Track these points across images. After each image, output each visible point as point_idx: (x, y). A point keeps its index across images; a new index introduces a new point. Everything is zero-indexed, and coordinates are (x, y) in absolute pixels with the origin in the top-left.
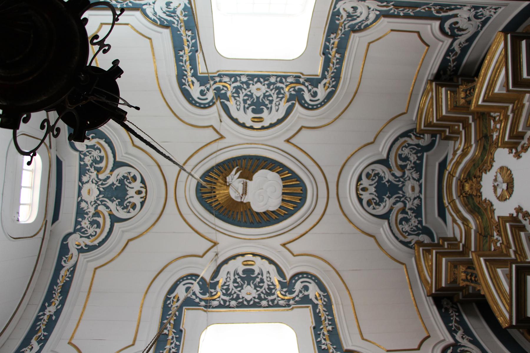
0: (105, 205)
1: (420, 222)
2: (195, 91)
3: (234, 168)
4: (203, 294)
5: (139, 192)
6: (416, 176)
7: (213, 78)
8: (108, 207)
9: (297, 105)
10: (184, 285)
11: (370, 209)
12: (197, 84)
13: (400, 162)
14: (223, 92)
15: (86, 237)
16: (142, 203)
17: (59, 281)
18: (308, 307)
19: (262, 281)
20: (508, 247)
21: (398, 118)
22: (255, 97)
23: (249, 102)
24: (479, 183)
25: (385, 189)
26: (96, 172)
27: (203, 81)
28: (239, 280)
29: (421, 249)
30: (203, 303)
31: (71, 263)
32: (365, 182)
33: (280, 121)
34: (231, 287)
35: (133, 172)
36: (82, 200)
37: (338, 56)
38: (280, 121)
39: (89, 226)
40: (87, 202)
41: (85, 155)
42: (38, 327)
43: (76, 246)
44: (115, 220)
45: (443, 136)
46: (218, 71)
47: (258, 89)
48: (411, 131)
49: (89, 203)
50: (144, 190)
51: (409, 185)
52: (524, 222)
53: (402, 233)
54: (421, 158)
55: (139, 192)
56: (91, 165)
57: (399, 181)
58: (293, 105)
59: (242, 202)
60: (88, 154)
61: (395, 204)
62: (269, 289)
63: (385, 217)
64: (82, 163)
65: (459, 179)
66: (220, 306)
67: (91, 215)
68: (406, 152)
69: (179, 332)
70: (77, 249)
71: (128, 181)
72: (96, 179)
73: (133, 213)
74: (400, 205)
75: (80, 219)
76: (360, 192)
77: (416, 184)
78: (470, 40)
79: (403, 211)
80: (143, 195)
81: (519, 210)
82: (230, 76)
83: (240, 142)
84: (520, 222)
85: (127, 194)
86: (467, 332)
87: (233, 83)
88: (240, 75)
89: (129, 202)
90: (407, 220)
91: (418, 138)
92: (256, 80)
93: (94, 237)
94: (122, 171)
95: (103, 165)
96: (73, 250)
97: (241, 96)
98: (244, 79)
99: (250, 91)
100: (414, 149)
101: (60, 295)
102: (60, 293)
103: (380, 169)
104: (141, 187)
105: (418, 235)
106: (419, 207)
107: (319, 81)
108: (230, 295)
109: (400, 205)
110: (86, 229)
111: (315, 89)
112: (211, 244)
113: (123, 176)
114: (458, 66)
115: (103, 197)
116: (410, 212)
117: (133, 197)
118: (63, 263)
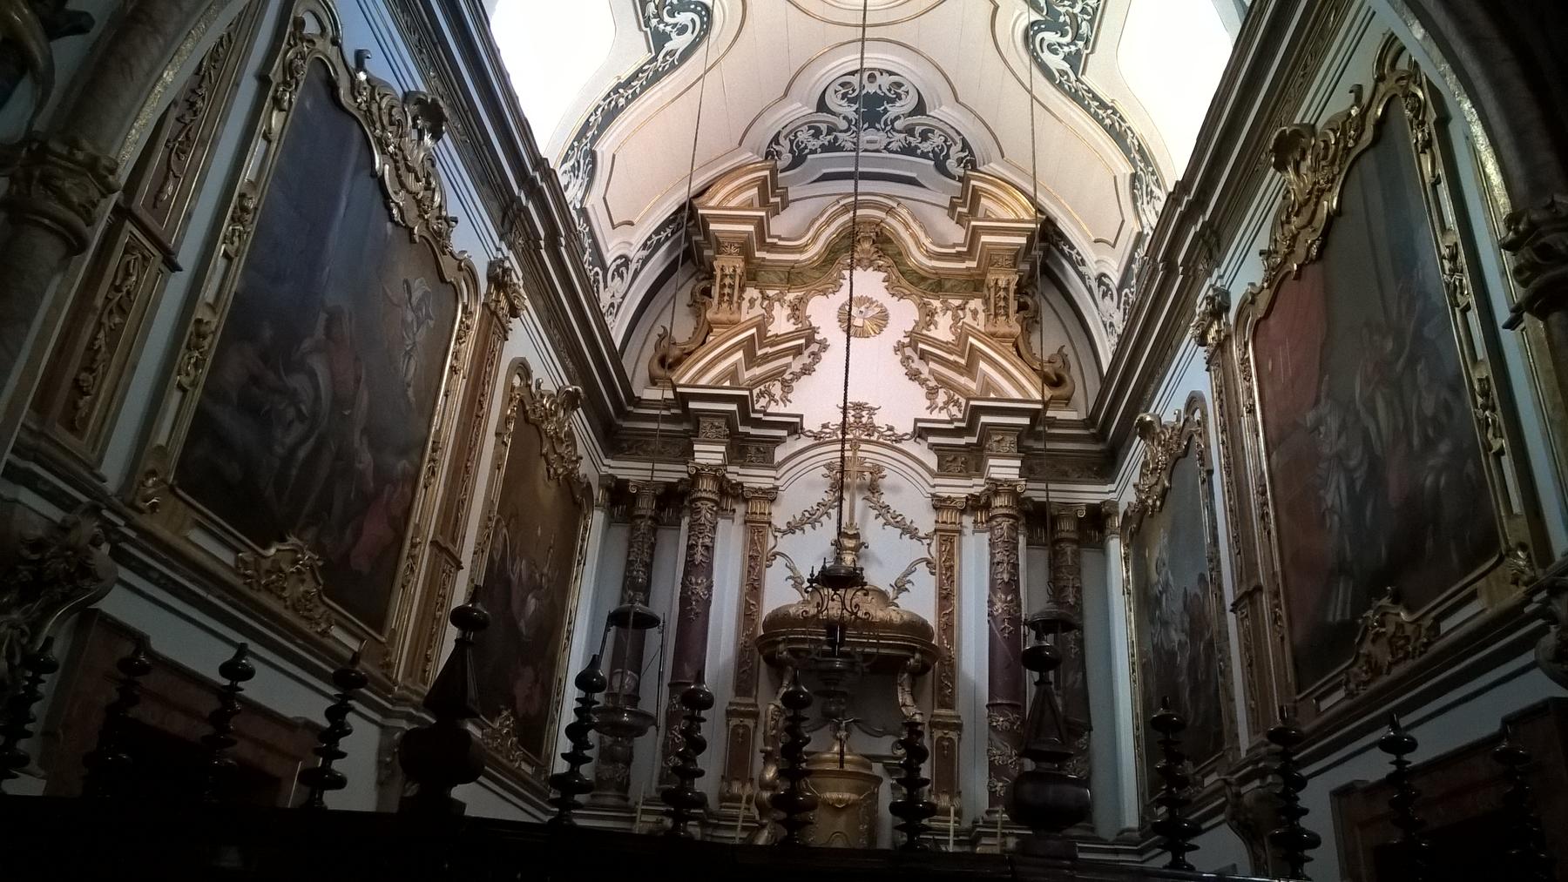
1: (813, 152)
9: (1035, 17)
11: (836, 86)
13: (918, 129)
25: (871, 109)
29: (767, 173)
32: (885, 81)
37: (1108, 121)
51: (880, 138)
52: (806, 353)
53: (795, 132)
54: (924, 155)
58: (1039, 10)
63: (822, 106)
68: (937, 140)
74: (843, 125)
81: (824, 346)
84: (807, 346)
86: (645, 261)
90: (817, 133)
91: (960, 161)
103: (909, 103)
105: (791, 151)
106: (840, 149)
107: (1074, 68)
109: (843, 125)
111: (1062, 55)
114: (1062, 252)
116: (830, 137)
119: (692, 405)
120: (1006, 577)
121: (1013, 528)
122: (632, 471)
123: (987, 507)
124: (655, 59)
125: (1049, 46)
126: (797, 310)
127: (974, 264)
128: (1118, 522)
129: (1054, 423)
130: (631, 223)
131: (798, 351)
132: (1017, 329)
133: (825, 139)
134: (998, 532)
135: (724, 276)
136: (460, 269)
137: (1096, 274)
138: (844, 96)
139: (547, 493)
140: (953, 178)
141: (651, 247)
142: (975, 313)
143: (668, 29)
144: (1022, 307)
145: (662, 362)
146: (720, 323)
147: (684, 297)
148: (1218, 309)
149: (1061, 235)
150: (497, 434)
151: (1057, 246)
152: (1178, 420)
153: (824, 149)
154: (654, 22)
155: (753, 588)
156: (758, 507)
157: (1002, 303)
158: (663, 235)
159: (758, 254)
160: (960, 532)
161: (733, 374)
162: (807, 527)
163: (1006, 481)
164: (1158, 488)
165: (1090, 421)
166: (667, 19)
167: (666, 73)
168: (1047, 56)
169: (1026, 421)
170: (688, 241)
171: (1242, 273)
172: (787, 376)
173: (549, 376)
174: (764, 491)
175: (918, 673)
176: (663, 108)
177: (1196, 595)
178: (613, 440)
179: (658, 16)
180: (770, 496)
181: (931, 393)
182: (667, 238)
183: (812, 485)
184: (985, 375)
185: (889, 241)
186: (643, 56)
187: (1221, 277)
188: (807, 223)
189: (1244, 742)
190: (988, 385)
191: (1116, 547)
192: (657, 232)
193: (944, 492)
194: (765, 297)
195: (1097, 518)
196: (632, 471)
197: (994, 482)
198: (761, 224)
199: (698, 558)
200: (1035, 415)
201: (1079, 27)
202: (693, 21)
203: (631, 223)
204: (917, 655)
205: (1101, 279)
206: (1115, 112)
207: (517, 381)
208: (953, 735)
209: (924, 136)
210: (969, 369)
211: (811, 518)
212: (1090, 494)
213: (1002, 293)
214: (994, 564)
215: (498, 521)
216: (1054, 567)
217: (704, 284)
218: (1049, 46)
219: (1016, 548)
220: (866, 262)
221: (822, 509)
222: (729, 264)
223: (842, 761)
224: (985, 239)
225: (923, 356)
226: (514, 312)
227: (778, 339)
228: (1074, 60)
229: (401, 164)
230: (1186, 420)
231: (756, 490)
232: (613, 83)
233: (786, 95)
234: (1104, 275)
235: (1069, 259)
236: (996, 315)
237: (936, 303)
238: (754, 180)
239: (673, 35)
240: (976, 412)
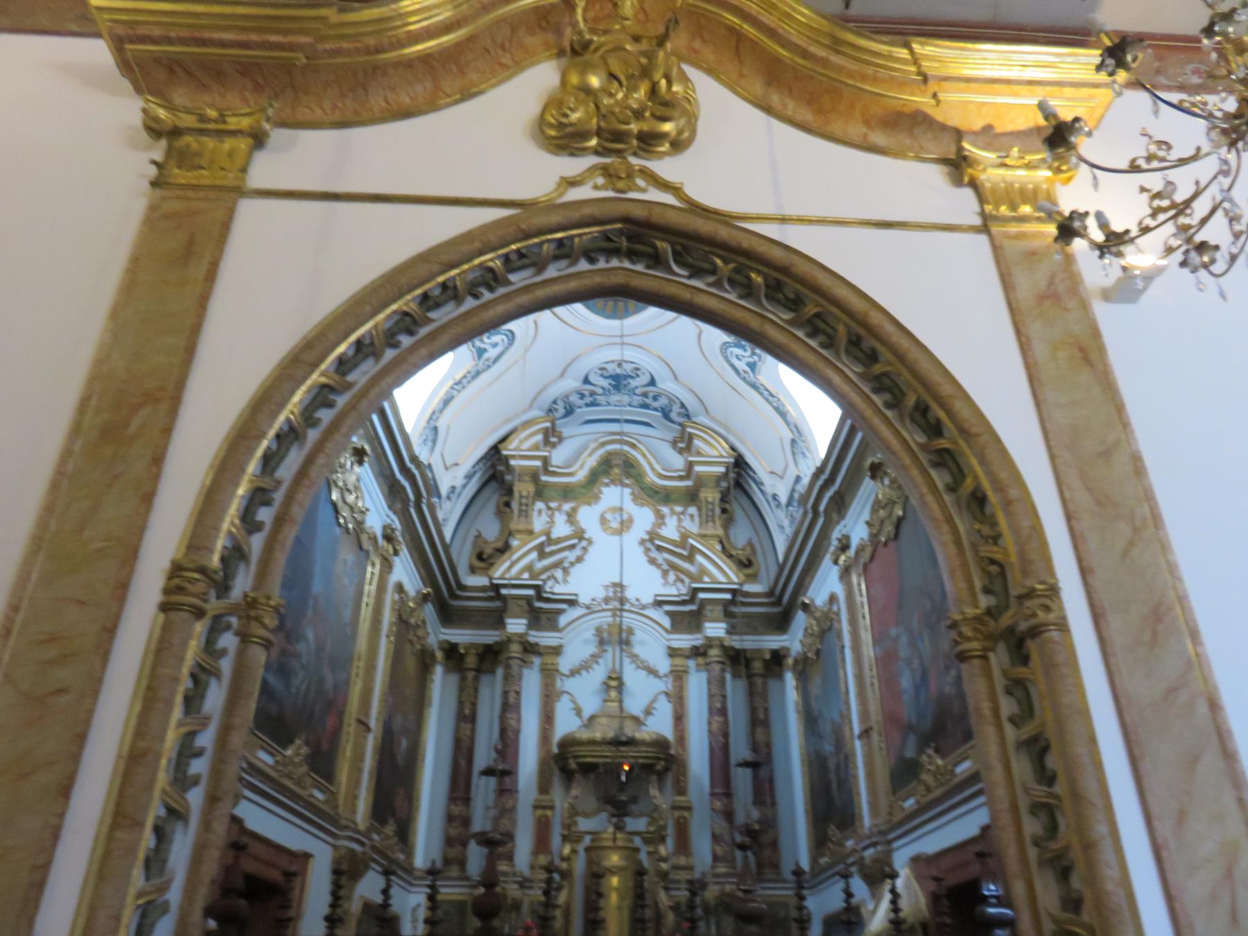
6: (635, 403)
13: (651, 395)
25: (618, 382)
29: (548, 424)
51: (626, 399)
52: (578, 548)
53: (567, 396)
54: (655, 409)
63: (586, 381)
74: (600, 391)
79: (592, 394)
86: (464, 486)
90: (582, 396)
91: (679, 414)
103: (645, 379)
106: (598, 405)
109: (600, 391)
119: (504, 591)
121: (723, 670)
122: (461, 636)
123: (704, 654)
126: (571, 517)
127: (689, 483)
128: (790, 661)
129: (748, 594)
130: (457, 464)
131: (573, 547)
132: (720, 532)
133: (588, 400)
135: (521, 497)
138: (602, 375)
140: (673, 422)
141: (469, 477)
142: (692, 516)
144: (724, 511)
145: (480, 557)
147: (491, 507)
153: (587, 405)
155: (548, 718)
156: (549, 659)
160: (686, 672)
161: (529, 568)
162: (584, 672)
165: (770, 594)
167: (484, 371)
169: (728, 596)
170: (495, 471)
171: (856, 527)
172: (566, 565)
174: (551, 647)
175: (661, 775)
178: (448, 615)
180: (557, 651)
181: (665, 574)
183: (586, 641)
185: (632, 466)
188: (576, 453)
189: (867, 821)
190: (703, 571)
191: (790, 679)
193: (675, 644)
194: (549, 508)
195: (777, 658)
196: (461, 636)
197: (709, 639)
198: (546, 461)
203: (457, 464)
204: (663, 761)
205: (775, 497)
208: (686, 814)
209: (655, 398)
210: (690, 559)
211: (585, 666)
212: (773, 642)
214: (711, 696)
216: (751, 694)
217: (506, 498)
222: (523, 488)
223: (615, 839)
224: (698, 468)
225: (659, 548)
226: (396, 553)
227: (560, 540)
235: (754, 479)
237: (665, 510)
240: (695, 591)
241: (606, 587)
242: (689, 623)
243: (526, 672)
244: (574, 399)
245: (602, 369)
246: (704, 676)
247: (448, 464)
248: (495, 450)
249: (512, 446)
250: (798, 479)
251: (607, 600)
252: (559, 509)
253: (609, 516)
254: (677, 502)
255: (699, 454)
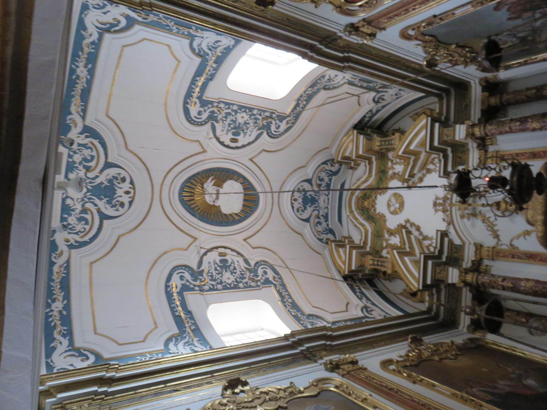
0: (93, 203)
1: (328, 225)
2: (194, 110)
3: (209, 177)
4: (195, 280)
5: (127, 193)
7: (211, 103)
8: (96, 205)
9: (265, 134)
10: (177, 274)
11: (298, 214)
12: (198, 104)
13: (319, 182)
14: (216, 115)
15: (74, 233)
16: (131, 203)
17: (54, 278)
18: (271, 286)
19: (235, 268)
20: (404, 244)
21: (322, 152)
22: (237, 123)
23: (232, 126)
24: (374, 201)
25: (309, 201)
26: (84, 171)
27: (204, 103)
28: (218, 268)
29: (333, 244)
30: (197, 288)
31: (63, 259)
33: (249, 144)
34: (214, 274)
35: (123, 174)
36: (67, 197)
37: (305, 103)
38: (249, 144)
39: (76, 222)
40: (72, 199)
41: (75, 153)
42: (53, 324)
43: (65, 243)
44: (104, 217)
45: (349, 167)
46: (219, 99)
47: (243, 117)
48: (328, 161)
49: (75, 200)
50: (132, 191)
52: (410, 229)
54: (330, 180)
55: (127, 193)
56: (80, 163)
57: (316, 195)
58: (262, 133)
59: (214, 205)
60: (78, 151)
61: (313, 211)
62: (241, 274)
63: (307, 220)
64: (70, 160)
65: (357, 197)
66: (210, 290)
67: (77, 211)
69: (189, 313)
70: (67, 245)
71: (118, 181)
72: (84, 177)
73: (122, 211)
75: (66, 216)
76: (293, 202)
77: (326, 197)
78: (384, 107)
79: (318, 217)
80: (131, 195)
81: (407, 221)
82: (226, 104)
83: (216, 156)
85: (116, 194)
87: (226, 109)
88: (233, 104)
89: (118, 201)
90: (319, 223)
91: (332, 165)
92: (243, 110)
93: (83, 234)
94: (112, 172)
95: (93, 164)
96: (62, 246)
97: (228, 120)
98: (235, 108)
99: (236, 118)
100: (327, 173)
101: (60, 291)
102: (60, 288)
103: (307, 186)
104: (130, 188)
105: (327, 234)
106: (327, 214)
107: (285, 118)
108: (215, 280)
110: (74, 225)
111: (280, 124)
112: (192, 240)
113: (113, 177)
114: (368, 121)
115: (91, 195)
116: (322, 218)
117: (121, 196)
118: (53, 260)
119: (429, 282)
120: (518, 123)
124: (275, 285)
125: (277, 128)
130: (348, 304)
131: (409, 233)
133: (322, 220)
134: (493, 131)
135: (374, 264)
136: (316, 386)
137: (374, 104)
138: (303, 211)
139: (464, 361)
140: (339, 169)
141: (362, 296)
143: (264, 278)
146: (393, 266)
147: (387, 283)
148: (353, 28)
149: (361, 122)
150: (414, 383)
151: (366, 124)
152: (419, 45)
154: (259, 283)
157: (387, 143)
158: (358, 290)
159: (368, 249)
161: (416, 263)
163: (467, 130)
164: (459, 50)
166: (259, 278)
168: (282, 129)
169: (437, 125)
172: (421, 238)
173: (398, 351)
174: (477, 249)
176: (298, 284)
177: (508, 10)
179: (257, 281)
182: (360, 289)
183: (473, 226)
184: (416, 146)
186: (273, 290)
187: (340, 31)
188: (355, 229)
190: (422, 144)
191: (503, 75)
192: (355, 293)
194: (386, 247)
195: (491, 87)
197: (467, 136)
198: (354, 247)
199: (510, 285)
200: (434, 121)
201: (267, 117)
202: (262, 268)
206: (299, 100)
207: (392, 367)
209: (322, 180)
210: (416, 154)
211: (491, 228)
212: (476, 92)
213: (383, 143)
214: (511, 131)
215: (467, 393)
216: (518, 103)
218: (277, 128)
219: (502, 121)
220: (373, 203)
221: (486, 221)
222: (369, 263)
224: (361, 152)
225: (412, 176)
226: (354, 363)
227: (403, 242)
228: (281, 118)
229: (246, 405)
230: (416, 39)
231: (476, 254)
232: (280, 303)
233: (300, 234)
234: (374, 100)
235: (371, 117)
236: (392, 144)
238: (335, 248)
239: (267, 276)
240: (432, 147)
241: (436, 211)
242: (461, 152)
243: (494, 272)
244: (320, 228)
245: (298, 211)
246: (500, 138)
247: (345, 310)
248: (346, 278)
249: (343, 266)
250: (350, 83)
251: (444, 211)
252: (387, 240)
253: (392, 209)
254: (385, 165)
255: (351, 153)
